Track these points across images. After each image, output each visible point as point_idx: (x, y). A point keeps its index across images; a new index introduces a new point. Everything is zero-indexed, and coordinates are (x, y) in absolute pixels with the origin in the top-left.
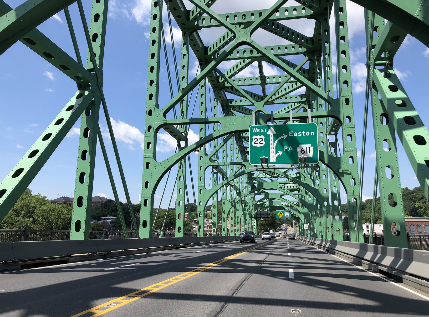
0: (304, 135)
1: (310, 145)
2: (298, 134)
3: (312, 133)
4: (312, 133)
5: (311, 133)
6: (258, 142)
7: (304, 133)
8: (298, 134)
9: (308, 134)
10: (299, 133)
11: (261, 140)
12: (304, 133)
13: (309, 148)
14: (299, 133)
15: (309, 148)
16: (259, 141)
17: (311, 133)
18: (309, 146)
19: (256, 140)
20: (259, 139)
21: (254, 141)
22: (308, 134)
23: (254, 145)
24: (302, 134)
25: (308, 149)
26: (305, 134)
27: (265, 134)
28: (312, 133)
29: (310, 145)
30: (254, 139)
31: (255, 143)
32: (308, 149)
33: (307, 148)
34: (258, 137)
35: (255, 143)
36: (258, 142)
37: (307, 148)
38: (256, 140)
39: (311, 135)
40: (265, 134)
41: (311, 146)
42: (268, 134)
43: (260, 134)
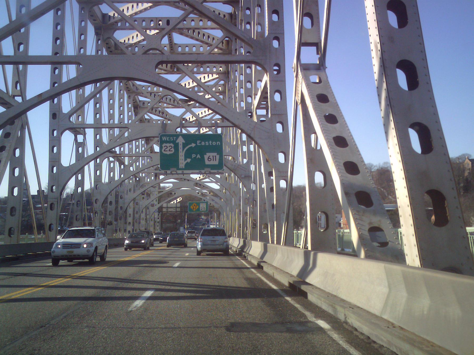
0: (211, 144)
1: (216, 154)
2: (205, 144)
3: (218, 143)
4: (218, 143)
5: (218, 143)
6: (168, 149)
7: (210, 142)
8: (205, 144)
9: (214, 143)
10: (206, 143)
11: (171, 147)
12: (210, 142)
13: (215, 156)
14: (206, 143)
15: (215, 156)
16: (169, 148)
17: (218, 143)
18: (215, 154)
19: (166, 147)
20: (169, 147)
21: (164, 148)
22: (214, 143)
23: (164, 153)
24: (209, 143)
25: (214, 157)
26: (212, 143)
27: (174, 142)
28: (218, 143)
29: (216, 154)
30: (164, 147)
31: (164, 151)
32: (214, 157)
33: (213, 156)
34: (168, 145)
35: (164, 151)
36: (168, 149)
37: (213, 156)
38: (166, 147)
39: (217, 144)
40: (174, 142)
41: (217, 154)
42: (177, 142)
43: (170, 142)
